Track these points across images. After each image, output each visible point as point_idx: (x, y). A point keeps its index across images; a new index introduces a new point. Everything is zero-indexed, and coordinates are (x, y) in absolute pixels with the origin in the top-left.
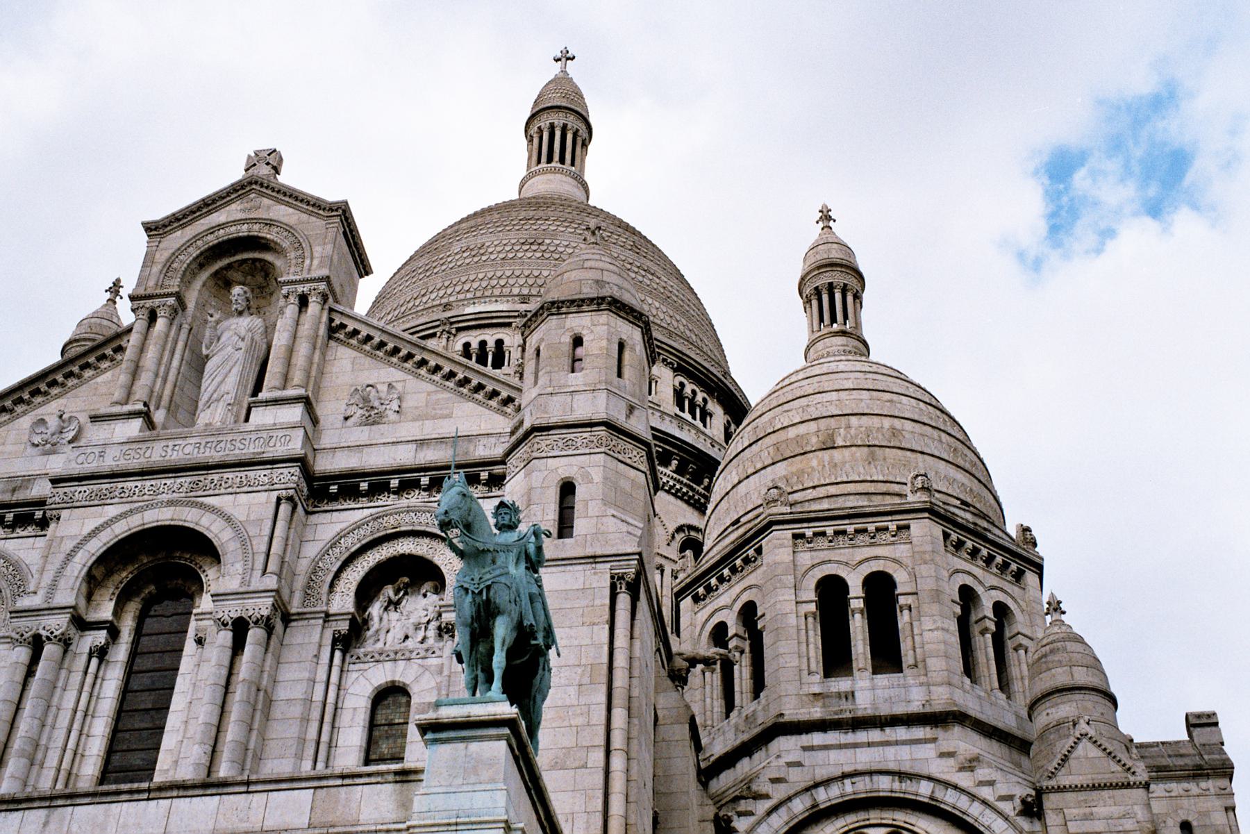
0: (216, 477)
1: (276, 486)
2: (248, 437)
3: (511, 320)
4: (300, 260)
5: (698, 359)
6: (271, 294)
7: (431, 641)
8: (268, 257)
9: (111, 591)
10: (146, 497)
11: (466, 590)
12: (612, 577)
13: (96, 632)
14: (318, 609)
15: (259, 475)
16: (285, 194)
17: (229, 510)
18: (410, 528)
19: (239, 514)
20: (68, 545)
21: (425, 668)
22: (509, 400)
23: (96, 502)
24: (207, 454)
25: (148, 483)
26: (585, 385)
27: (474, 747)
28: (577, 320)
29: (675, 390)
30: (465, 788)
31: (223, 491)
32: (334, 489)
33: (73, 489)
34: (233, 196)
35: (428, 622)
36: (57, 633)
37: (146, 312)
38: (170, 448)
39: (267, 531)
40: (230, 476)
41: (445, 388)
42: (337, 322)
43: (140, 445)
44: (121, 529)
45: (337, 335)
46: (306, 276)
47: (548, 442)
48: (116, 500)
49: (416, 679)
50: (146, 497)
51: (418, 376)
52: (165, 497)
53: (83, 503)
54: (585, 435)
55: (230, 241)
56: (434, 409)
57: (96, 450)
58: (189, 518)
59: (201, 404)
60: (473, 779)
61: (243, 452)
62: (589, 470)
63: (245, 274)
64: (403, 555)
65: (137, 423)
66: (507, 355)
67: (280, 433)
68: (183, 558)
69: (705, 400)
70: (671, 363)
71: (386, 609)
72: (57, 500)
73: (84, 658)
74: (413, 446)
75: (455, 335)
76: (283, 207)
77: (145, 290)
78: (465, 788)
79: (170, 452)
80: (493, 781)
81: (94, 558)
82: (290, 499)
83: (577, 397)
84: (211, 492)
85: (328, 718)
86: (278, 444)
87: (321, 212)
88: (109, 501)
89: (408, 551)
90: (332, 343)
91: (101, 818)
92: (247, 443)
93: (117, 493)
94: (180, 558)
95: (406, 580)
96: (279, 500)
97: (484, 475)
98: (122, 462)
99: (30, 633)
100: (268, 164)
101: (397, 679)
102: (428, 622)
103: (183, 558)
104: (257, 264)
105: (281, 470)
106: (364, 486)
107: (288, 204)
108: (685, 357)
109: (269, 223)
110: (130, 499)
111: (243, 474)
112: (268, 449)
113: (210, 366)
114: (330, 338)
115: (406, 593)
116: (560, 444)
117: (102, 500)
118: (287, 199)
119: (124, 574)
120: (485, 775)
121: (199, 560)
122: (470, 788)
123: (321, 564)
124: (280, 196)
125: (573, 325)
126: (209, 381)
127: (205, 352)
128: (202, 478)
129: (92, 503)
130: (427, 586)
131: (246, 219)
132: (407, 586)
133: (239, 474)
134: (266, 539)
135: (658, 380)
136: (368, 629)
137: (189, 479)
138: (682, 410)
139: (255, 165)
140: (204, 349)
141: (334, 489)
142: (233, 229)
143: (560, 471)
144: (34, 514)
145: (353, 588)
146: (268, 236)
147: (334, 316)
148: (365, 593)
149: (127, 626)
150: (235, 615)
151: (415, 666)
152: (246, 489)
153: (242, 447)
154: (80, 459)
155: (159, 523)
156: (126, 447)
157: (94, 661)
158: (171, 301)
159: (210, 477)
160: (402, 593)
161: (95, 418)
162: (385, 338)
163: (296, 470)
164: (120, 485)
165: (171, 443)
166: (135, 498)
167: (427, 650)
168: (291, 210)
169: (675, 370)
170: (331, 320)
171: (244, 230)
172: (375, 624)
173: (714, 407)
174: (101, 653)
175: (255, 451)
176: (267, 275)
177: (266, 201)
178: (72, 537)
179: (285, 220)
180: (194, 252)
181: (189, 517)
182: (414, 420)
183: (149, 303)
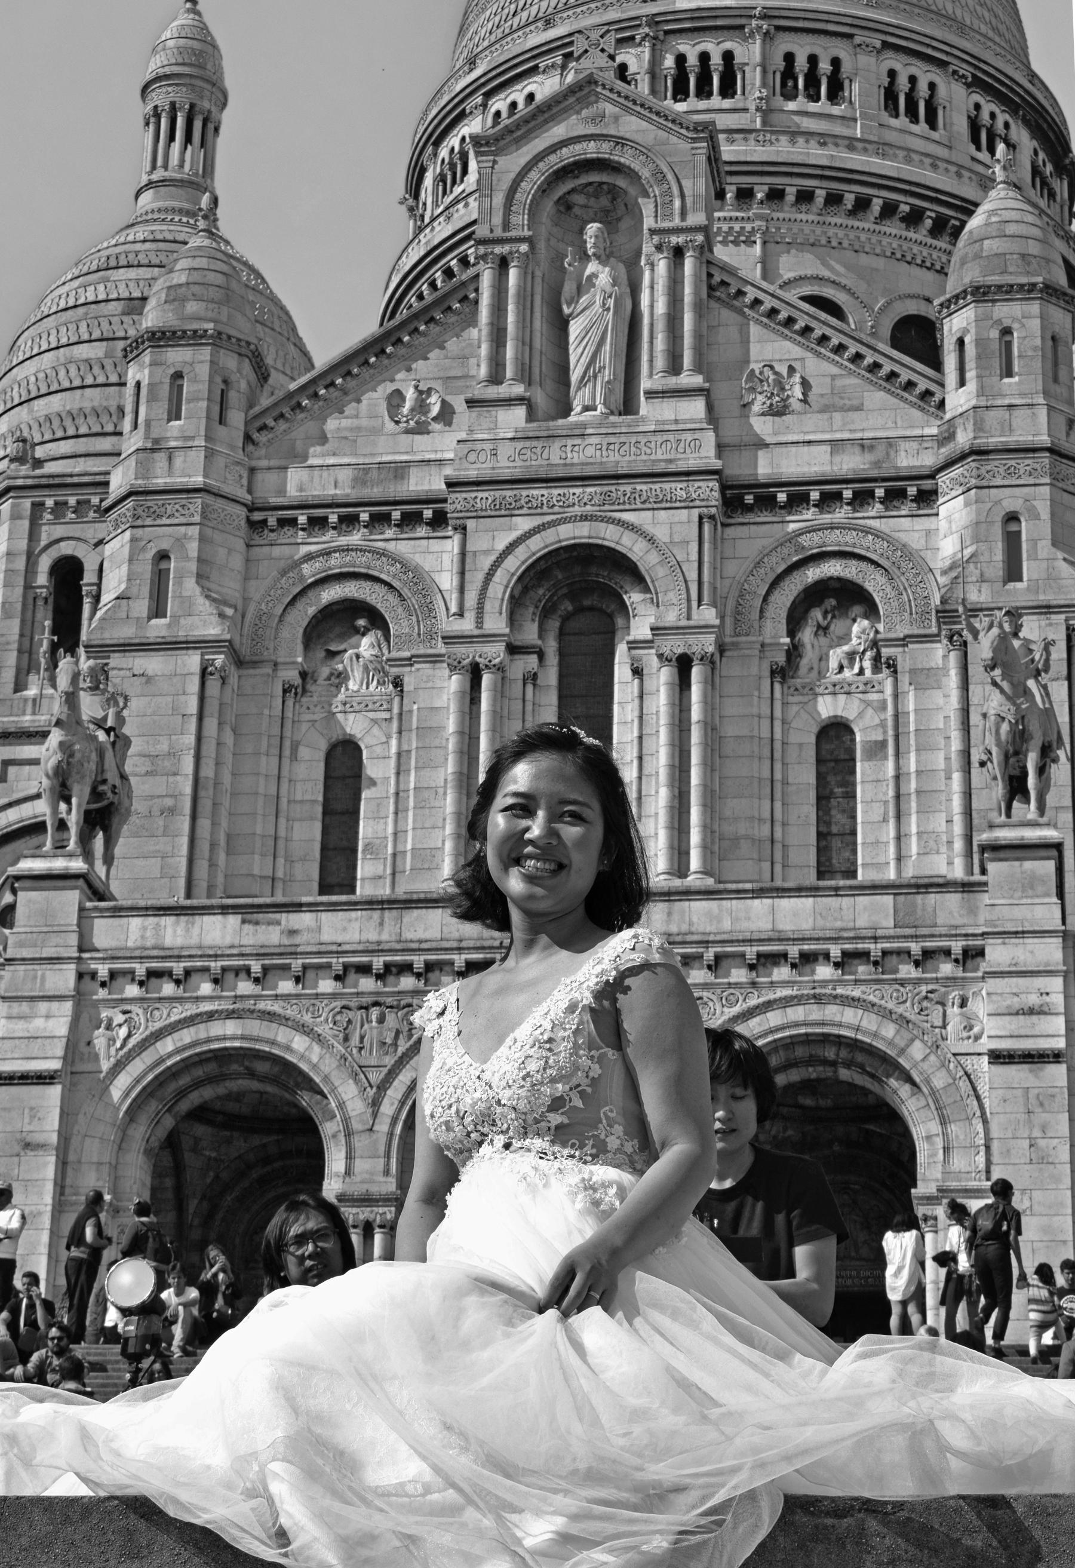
0: (628, 489)
1: (697, 503)
2: (652, 438)
3: (743, 21)
4: (668, 199)
5: (1000, 65)
6: (619, 220)
7: (868, 673)
8: (621, 182)
9: (531, 610)
10: (556, 509)
11: (1003, 719)
12: (1068, 629)
13: (526, 656)
14: (753, 639)
15: (678, 488)
16: (635, 102)
17: (649, 529)
18: (836, 548)
19: (661, 534)
20: (487, 562)
21: (868, 704)
22: (927, 394)
23: (503, 512)
24: (612, 459)
25: (556, 492)
26: (1022, 395)
27: (1028, 865)
28: (1005, 309)
29: (969, 117)
30: (1024, 901)
31: (639, 506)
32: (749, 499)
33: (473, 495)
34: (571, 100)
35: (864, 652)
36: (494, 662)
37: (497, 262)
38: (569, 449)
39: (694, 556)
40: (644, 487)
41: (851, 373)
42: (717, 279)
43: (535, 443)
44: (537, 545)
45: (718, 294)
46: (677, 222)
47: (988, 468)
48: (525, 511)
49: (861, 715)
50: (556, 509)
51: (818, 354)
52: (577, 510)
53: (489, 513)
54: (1027, 462)
55: (575, 163)
56: (842, 398)
57: (488, 446)
58: (607, 536)
59: (575, 377)
60: (1030, 892)
61: (653, 457)
62: (1035, 503)
63: (588, 195)
64: (831, 578)
65: (521, 412)
66: (739, 77)
67: (689, 436)
68: (602, 575)
69: (1007, 125)
70: (963, 76)
71: (816, 634)
72: (459, 507)
73: (520, 683)
74: (827, 448)
75: (662, 41)
76: (633, 118)
77: (492, 231)
78: (1024, 901)
79: (569, 455)
80: (1047, 895)
81: (515, 578)
82: (712, 517)
83: (1017, 413)
84: (627, 507)
85: (778, 755)
86: (688, 451)
87: (683, 131)
88: (517, 512)
89: (836, 574)
90: (713, 304)
91: (716, 911)
92: (653, 445)
93: (523, 502)
94: (597, 575)
95: (834, 602)
96: (701, 518)
97: (912, 491)
98: (519, 463)
99: (467, 661)
100: (603, 50)
101: (839, 713)
102: (864, 652)
103: (602, 575)
104: (605, 187)
105: (697, 484)
106: (782, 497)
107: (639, 115)
108: (982, 65)
109: (620, 142)
110: (539, 511)
111: (657, 486)
112: (679, 456)
113: (575, 329)
114: (709, 296)
115: (834, 617)
116: (1002, 470)
117: (507, 511)
118: (638, 109)
119: (541, 592)
120: (1040, 889)
121: (618, 578)
122: (1029, 901)
123: (746, 586)
124: (630, 104)
125: (1002, 315)
126: (580, 350)
127: (566, 310)
128: (613, 488)
129: (497, 513)
130: (857, 609)
131: (592, 135)
132: (834, 608)
133: (654, 487)
134: (696, 565)
135: (948, 105)
136: (800, 656)
137: (598, 489)
138: (979, 148)
139: (586, 51)
140: (565, 307)
141: (749, 499)
142: (578, 148)
143: (1005, 503)
144: (421, 513)
145: (784, 614)
146: (622, 160)
147: (714, 271)
148: (795, 621)
149: (551, 647)
150: (679, 651)
151: (856, 702)
152: (664, 505)
153: (648, 451)
154: (472, 457)
155: (577, 541)
156: (520, 445)
157: (530, 688)
158: (524, 248)
159: (622, 488)
160: (829, 616)
161: (471, 403)
162: (776, 304)
163: (715, 485)
164: (524, 493)
165: (570, 442)
166: (545, 509)
167: (866, 684)
168: (644, 124)
169: (968, 85)
170: (710, 275)
171: (591, 150)
172: (809, 656)
173: (1021, 135)
174: (532, 678)
175: (665, 457)
176: (614, 199)
177: (610, 109)
178: (486, 552)
179: (638, 138)
180: (536, 177)
181: (609, 536)
182: (821, 411)
183: (498, 250)
